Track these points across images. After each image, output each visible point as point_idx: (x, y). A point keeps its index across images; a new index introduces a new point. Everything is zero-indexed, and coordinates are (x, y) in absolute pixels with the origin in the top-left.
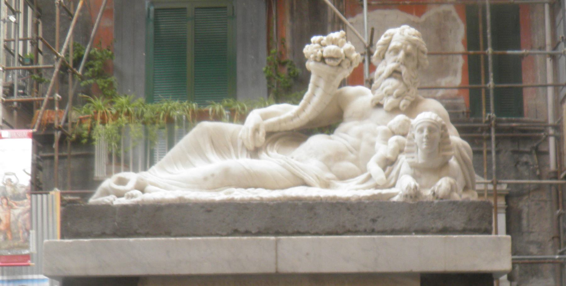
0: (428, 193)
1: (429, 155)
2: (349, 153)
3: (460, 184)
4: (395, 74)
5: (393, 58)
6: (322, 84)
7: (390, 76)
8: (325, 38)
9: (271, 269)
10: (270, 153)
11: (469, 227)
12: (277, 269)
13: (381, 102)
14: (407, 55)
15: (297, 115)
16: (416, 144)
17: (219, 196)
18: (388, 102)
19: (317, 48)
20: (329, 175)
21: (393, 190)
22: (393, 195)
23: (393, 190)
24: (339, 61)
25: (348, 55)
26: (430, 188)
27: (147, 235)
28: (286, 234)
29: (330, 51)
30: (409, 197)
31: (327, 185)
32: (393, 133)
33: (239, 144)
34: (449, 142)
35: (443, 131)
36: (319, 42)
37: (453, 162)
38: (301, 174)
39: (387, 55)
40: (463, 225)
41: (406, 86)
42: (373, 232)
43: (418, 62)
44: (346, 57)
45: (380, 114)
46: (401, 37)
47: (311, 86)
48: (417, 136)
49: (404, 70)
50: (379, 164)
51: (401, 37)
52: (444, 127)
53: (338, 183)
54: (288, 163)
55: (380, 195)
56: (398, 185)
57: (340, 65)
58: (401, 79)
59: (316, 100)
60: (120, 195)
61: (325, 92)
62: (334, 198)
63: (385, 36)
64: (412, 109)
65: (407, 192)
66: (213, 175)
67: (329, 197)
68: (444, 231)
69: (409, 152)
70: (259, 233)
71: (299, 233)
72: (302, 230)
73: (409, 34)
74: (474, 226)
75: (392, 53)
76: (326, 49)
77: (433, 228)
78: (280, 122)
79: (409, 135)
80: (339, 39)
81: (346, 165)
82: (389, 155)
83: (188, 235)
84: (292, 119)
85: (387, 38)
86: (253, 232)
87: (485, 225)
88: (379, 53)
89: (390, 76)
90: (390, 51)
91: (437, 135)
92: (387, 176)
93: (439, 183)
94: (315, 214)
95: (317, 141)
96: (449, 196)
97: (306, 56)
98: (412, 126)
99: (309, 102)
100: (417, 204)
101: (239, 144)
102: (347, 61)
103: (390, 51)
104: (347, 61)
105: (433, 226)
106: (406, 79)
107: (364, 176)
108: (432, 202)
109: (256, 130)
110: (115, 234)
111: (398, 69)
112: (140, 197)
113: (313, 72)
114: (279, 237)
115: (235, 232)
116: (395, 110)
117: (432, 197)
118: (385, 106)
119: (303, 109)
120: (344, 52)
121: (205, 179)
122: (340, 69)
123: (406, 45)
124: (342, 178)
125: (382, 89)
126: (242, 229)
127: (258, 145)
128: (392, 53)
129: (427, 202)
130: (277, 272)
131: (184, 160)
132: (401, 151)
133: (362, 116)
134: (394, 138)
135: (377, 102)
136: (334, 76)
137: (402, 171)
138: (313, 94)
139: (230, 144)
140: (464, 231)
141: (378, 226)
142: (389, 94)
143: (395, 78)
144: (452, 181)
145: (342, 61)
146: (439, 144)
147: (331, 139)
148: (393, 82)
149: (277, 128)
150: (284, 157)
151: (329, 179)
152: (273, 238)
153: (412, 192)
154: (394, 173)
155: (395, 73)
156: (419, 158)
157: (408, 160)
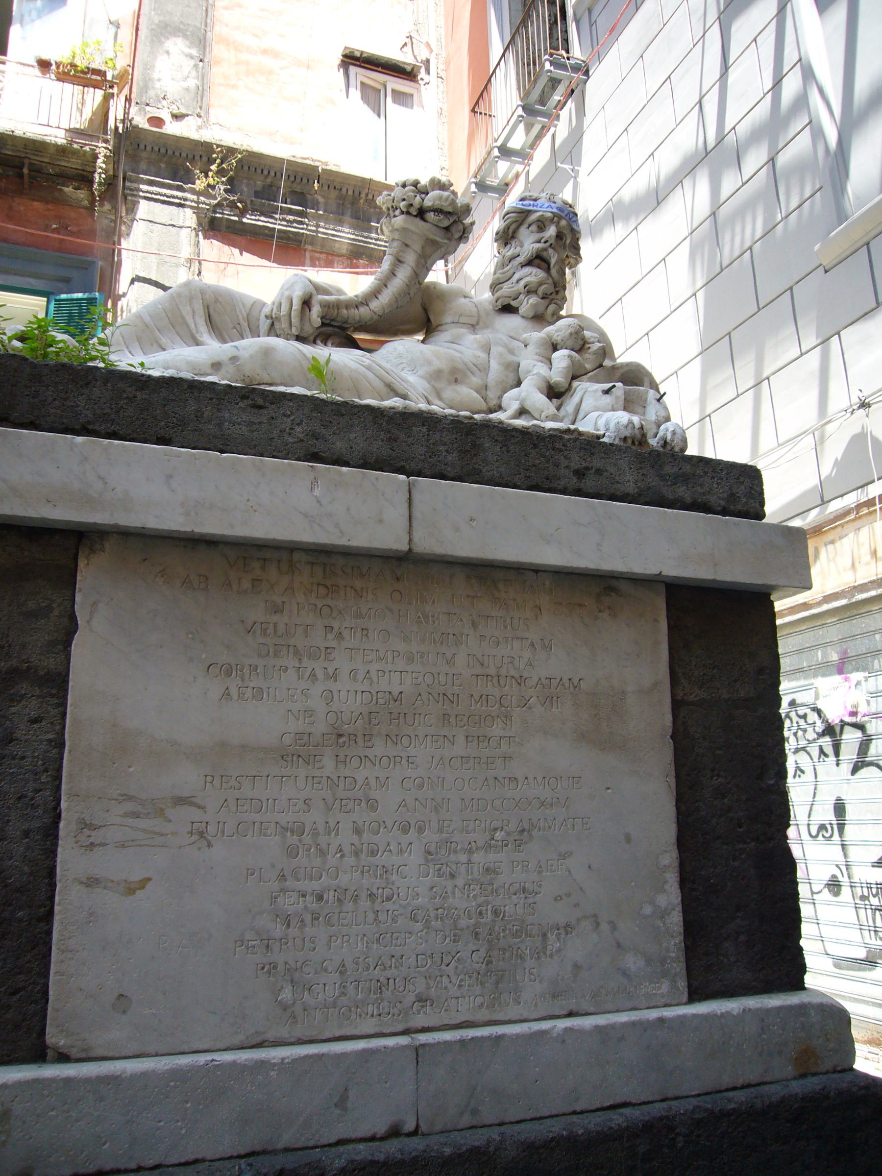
4: (537, 261)
5: (537, 236)
6: (410, 258)
7: (529, 263)
18: (527, 304)
30: (630, 441)
39: (523, 231)
40: (723, 503)
45: (511, 322)
58: (548, 270)
65: (628, 433)
89: (529, 263)
90: (530, 226)
94: (474, 446)
111: (545, 254)
118: (522, 310)
125: (518, 282)
128: (534, 228)
130: (410, 550)
132: (574, 378)
137: (584, 407)
142: (530, 291)
148: (534, 275)
152: (402, 477)
155: (538, 260)
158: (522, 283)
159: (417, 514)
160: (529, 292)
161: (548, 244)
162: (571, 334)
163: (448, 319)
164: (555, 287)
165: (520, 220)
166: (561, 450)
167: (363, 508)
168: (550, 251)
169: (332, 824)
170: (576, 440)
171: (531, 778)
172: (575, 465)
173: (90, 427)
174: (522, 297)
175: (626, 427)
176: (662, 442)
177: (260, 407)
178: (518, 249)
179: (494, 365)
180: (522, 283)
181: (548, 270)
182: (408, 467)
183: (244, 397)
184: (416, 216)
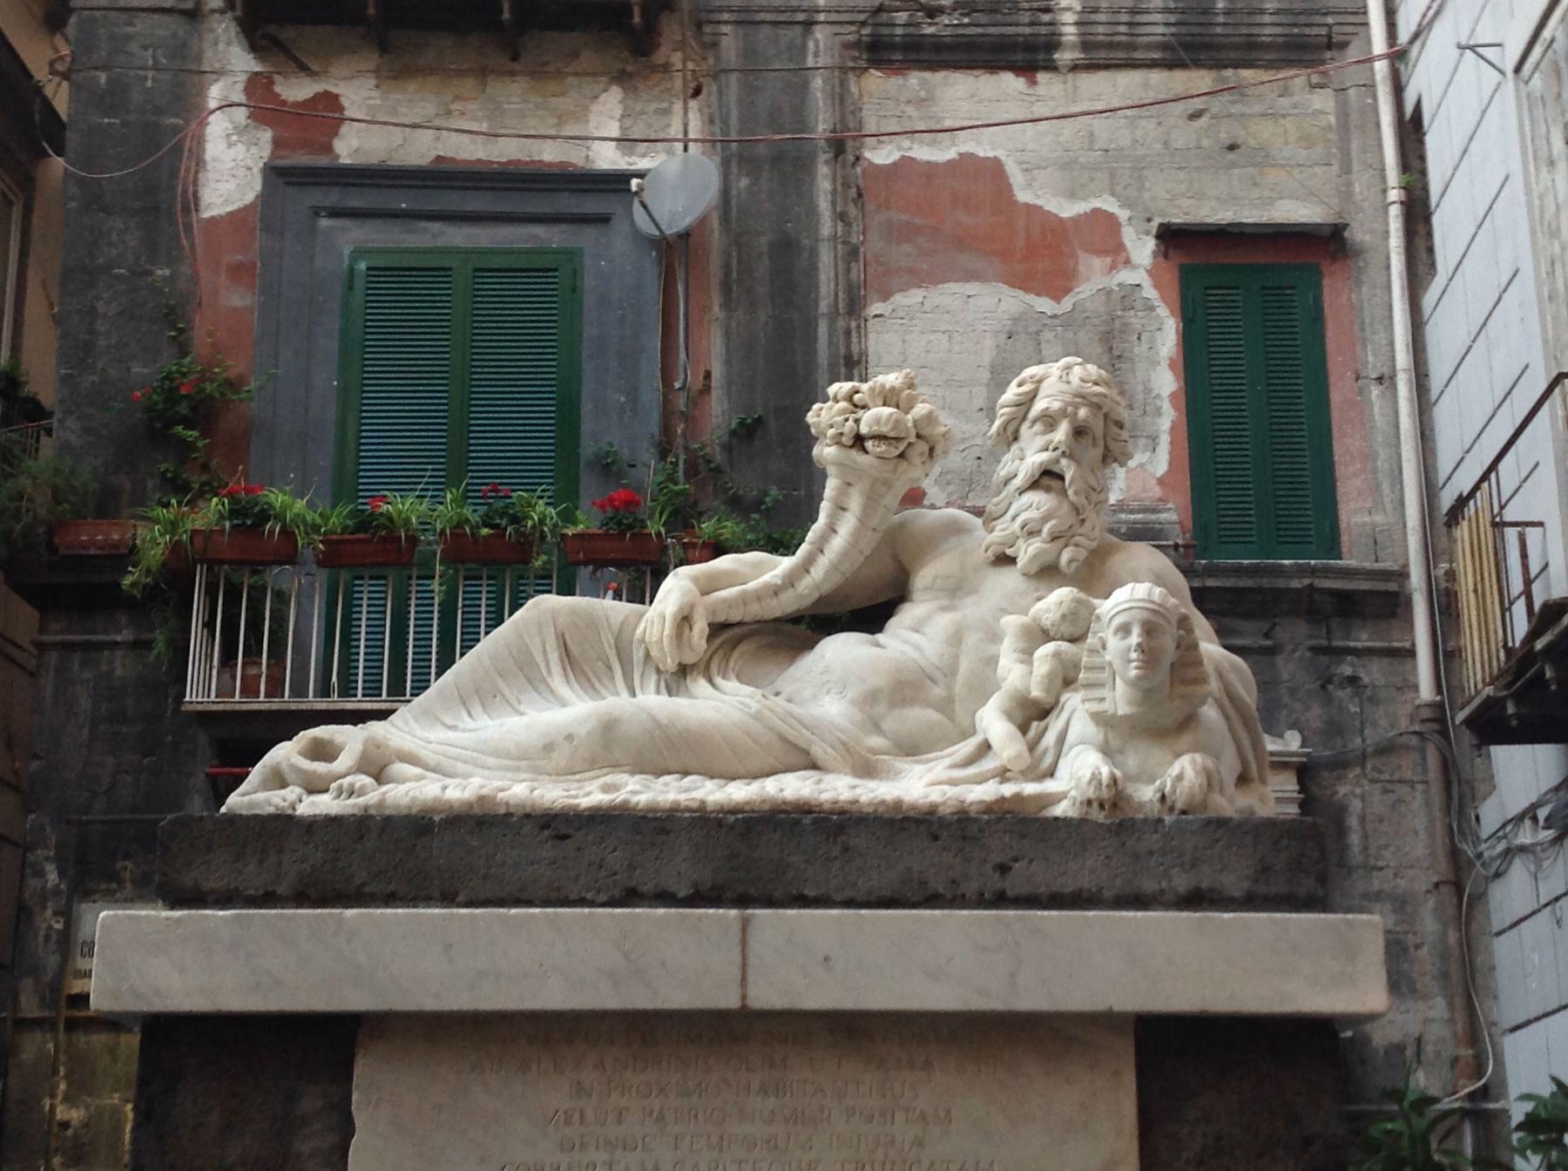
0: (1146, 793)
1: (1146, 692)
2: (928, 682)
3: (1229, 768)
5: (1040, 441)
6: (855, 503)
7: (1034, 485)
8: (865, 387)
9: (729, 1000)
10: (719, 680)
11: (1263, 889)
12: (744, 997)
13: (1009, 552)
14: (1079, 432)
15: (790, 580)
16: (1110, 664)
17: (590, 794)
18: (1027, 552)
19: (843, 411)
20: (876, 741)
21: (1050, 786)
22: (1055, 799)
23: (1050, 786)
24: (902, 447)
25: (924, 432)
26: (1152, 780)
27: (390, 900)
28: (771, 903)
29: (878, 421)
30: (1095, 805)
31: (867, 769)
32: (1046, 636)
33: (638, 655)
34: (1198, 662)
35: (1181, 632)
36: (850, 398)
37: (1210, 712)
40: (1246, 885)
41: (1077, 510)
42: (1000, 900)
43: (1106, 447)
46: (1064, 387)
47: (825, 508)
48: (1114, 643)
49: (1069, 470)
50: (1009, 715)
51: (1064, 387)
52: (1184, 622)
53: (900, 764)
54: (770, 710)
55: (1018, 797)
56: (1058, 774)
57: (902, 456)
59: (838, 543)
60: (315, 787)
61: (863, 520)
62: (898, 804)
63: (1020, 385)
64: (1093, 575)
65: (1091, 793)
67: (883, 802)
68: (1195, 900)
69: (1090, 686)
72: (810, 892)
74: (1276, 887)
75: (1038, 427)
76: (867, 417)
77: (1162, 891)
78: (744, 599)
79: (1091, 640)
80: (901, 390)
81: (919, 716)
82: (1036, 692)
84: (776, 591)
85: (1027, 388)
86: (682, 894)
87: (1308, 885)
88: (1005, 427)
89: (1034, 485)
90: (1034, 422)
91: (1168, 642)
92: (1032, 747)
93: (1175, 770)
94: (846, 850)
95: (842, 650)
96: (1204, 805)
97: (813, 431)
98: (1098, 618)
99: (820, 549)
100: (1121, 824)
101: (638, 655)
103: (1034, 422)
104: (923, 447)
105: (1164, 884)
106: (1076, 493)
107: (967, 747)
108: (1160, 821)
109: (684, 620)
110: (301, 899)
111: (1056, 469)
112: (373, 795)
113: (831, 470)
114: (749, 911)
115: (630, 897)
116: (1048, 573)
117: (1157, 806)
118: (1021, 562)
119: (805, 567)
120: (915, 422)
121: (549, 747)
122: (904, 465)
123: (1076, 407)
124: (912, 748)
125: (1014, 518)
127: (689, 659)
128: (1038, 427)
129: (1146, 820)
130: (744, 1007)
132: (1068, 683)
133: (956, 590)
134: (1050, 647)
135: (999, 549)
136: (887, 484)
138: (832, 529)
140: (1251, 902)
141: (1015, 885)
143: (1048, 489)
144: (1210, 763)
146: (1172, 664)
147: (878, 645)
148: (1038, 503)
149: (736, 617)
150: (759, 692)
152: (733, 912)
153: (1105, 794)
154: (1050, 739)
155: (1047, 478)
156: (1119, 699)
157: (1087, 705)
158: (1020, 520)
159: (752, 960)
160: (1031, 534)
161: (1058, 452)
162: (1064, 616)
164: (1078, 513)
166: (975, 839)
167: (681, 956)
168: (1064, 462)
170: (999, 820)
172: (997, 858)
173: (367, 889)
174: (1020, 542)
175: (1090, 783)
176: (1158, 795)
177: (565, 837)
178: (1017, 462)
179: (965, 664)
180: (1020, 520)
181: (1064, 492)
182: (752, 891)
183: (545, 826)
184: (851, 447)
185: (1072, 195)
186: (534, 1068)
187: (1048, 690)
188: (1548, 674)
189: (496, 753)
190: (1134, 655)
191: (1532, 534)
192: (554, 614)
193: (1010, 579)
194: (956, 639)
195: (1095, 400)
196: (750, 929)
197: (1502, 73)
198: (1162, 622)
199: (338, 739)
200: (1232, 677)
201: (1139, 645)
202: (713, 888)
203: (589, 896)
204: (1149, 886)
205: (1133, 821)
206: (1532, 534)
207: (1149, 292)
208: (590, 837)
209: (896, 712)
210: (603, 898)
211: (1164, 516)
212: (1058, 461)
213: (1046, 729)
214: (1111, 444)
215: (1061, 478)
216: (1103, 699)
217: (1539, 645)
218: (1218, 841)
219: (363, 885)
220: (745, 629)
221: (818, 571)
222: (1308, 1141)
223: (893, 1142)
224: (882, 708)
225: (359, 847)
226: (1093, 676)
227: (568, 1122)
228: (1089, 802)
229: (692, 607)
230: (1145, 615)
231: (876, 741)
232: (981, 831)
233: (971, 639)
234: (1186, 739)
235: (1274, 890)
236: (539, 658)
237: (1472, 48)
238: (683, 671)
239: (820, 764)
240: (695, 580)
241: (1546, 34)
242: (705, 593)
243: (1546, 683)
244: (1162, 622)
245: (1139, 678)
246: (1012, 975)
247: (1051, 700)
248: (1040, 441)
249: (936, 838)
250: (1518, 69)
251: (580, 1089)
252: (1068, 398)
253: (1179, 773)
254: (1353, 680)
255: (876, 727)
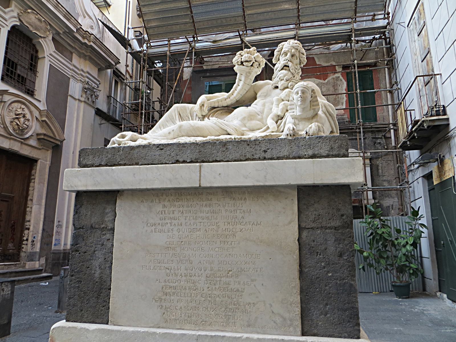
4: (285, 68)
6: (243, 78)
7: (282, 69)
13: (277, 85)
14: (292, 56)
20: (244, 129)
24: (251, 63)
25: (257, 60)
30: (289, 135)
32: (283, 100)
33: (195, 115)
36: (240, 54)
37: (320, 112)
38: (226, 128)
40: (327, 152)
44: (256, 61)
49: (290, 64)
50: (273, 119)
53: (249, 133)
57: (252, 66)
59: (239, 88)
65: (288, 133)
66: (173, 130)
68: (313, 156)
70: (191, 162)
71: (216, 161)
73: (293, 43)
75: (283, 56)
81: (254, 123)
82: (279, 113)
83: (148, 164)
86: (188, 161)
87: (343, 151)
91: (309, 95)
101: (195, 115)
102: (256, 63)
105: (306, 153)
108: (305, 138)
110: (106, 165)
111: (287, 65)
115: (177, 162)
122: (252, 67)
126: (181, 160)
127: (204, 114)
130: (200, 186)
131: (164, 126)
133: (266, 96)
136: (250, 73)
139: (189, 115)
141: (268, 155)
143: (286, 70)
145: (253, 63)
149: (216, 105)
151: (243, 131)
152: (198, 164)
155: (286, 67)
156: (298, 112)
159: (202, 175)
163: (258, 95)
165: (279, 54)
168: (289, 62)
169: (179, 268)
171: (242, 254)
172: (263, 149)
174: (279, 82)
179: (266, 110)
183: (158, 147)
185: (327, 62)
186: (154, 202)
187: (282, 112)
188: (415, 135)
189: (161, 136)
190: (299, 99)
191: (412, 112)
192: (177, 107)
193: (277, 90)
194: (264, 105)
195: (296, 47)
196: (201, 168)
197: (405, 27)
198: (306, 90)
199: (126, 134)
200: (328, 107)
201: (300, 96)
202: (195, 159)
203: (167, 162)
204: (301, 153)
205: (298, 138)
206: (412, 112)
207: (341, 78)
208: (168, 149)
209: (249, 122)
210: (171, 163)
211: (344, 116)
212: (287, 63)
213: (282, 122)
214: (301, 59)
215: (288, 67)
216: (294, 112)
217: (413, 129)
218: (319, 142)
219: (119, 162)
220: (219, 108)
221: (235, 94)
222: (342, 215)
223: (237, 218)
224: (245, 122)
225: (118, 153)
226: (291, 107)
227: (162, 214)
228: (288, 135)
229: (204, 102)
230: (302, 88)
231: (244, 129)
232: (260, 143)
233: (267, 105)
234: (314, 120)
235: (334, 153)
236: (174, 117)
237: (399, 24)
238: (204, 117)
239: (230, 133)
240: (206, 97)
241: (413, 17)
242: (208, 100)
243: (415, 137)
244: (306, 90)
245: (301, 104)
246: (265, 176)
247: (282, 115)
248: (284, 58)
249: (248, 145)
250: (408, 26)
251: (164, 206)
252: (289, 48)
253: (312, 127)
254: (380, 143)
255: (245, 126)
